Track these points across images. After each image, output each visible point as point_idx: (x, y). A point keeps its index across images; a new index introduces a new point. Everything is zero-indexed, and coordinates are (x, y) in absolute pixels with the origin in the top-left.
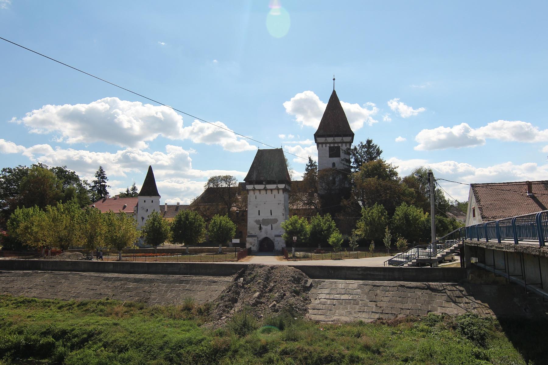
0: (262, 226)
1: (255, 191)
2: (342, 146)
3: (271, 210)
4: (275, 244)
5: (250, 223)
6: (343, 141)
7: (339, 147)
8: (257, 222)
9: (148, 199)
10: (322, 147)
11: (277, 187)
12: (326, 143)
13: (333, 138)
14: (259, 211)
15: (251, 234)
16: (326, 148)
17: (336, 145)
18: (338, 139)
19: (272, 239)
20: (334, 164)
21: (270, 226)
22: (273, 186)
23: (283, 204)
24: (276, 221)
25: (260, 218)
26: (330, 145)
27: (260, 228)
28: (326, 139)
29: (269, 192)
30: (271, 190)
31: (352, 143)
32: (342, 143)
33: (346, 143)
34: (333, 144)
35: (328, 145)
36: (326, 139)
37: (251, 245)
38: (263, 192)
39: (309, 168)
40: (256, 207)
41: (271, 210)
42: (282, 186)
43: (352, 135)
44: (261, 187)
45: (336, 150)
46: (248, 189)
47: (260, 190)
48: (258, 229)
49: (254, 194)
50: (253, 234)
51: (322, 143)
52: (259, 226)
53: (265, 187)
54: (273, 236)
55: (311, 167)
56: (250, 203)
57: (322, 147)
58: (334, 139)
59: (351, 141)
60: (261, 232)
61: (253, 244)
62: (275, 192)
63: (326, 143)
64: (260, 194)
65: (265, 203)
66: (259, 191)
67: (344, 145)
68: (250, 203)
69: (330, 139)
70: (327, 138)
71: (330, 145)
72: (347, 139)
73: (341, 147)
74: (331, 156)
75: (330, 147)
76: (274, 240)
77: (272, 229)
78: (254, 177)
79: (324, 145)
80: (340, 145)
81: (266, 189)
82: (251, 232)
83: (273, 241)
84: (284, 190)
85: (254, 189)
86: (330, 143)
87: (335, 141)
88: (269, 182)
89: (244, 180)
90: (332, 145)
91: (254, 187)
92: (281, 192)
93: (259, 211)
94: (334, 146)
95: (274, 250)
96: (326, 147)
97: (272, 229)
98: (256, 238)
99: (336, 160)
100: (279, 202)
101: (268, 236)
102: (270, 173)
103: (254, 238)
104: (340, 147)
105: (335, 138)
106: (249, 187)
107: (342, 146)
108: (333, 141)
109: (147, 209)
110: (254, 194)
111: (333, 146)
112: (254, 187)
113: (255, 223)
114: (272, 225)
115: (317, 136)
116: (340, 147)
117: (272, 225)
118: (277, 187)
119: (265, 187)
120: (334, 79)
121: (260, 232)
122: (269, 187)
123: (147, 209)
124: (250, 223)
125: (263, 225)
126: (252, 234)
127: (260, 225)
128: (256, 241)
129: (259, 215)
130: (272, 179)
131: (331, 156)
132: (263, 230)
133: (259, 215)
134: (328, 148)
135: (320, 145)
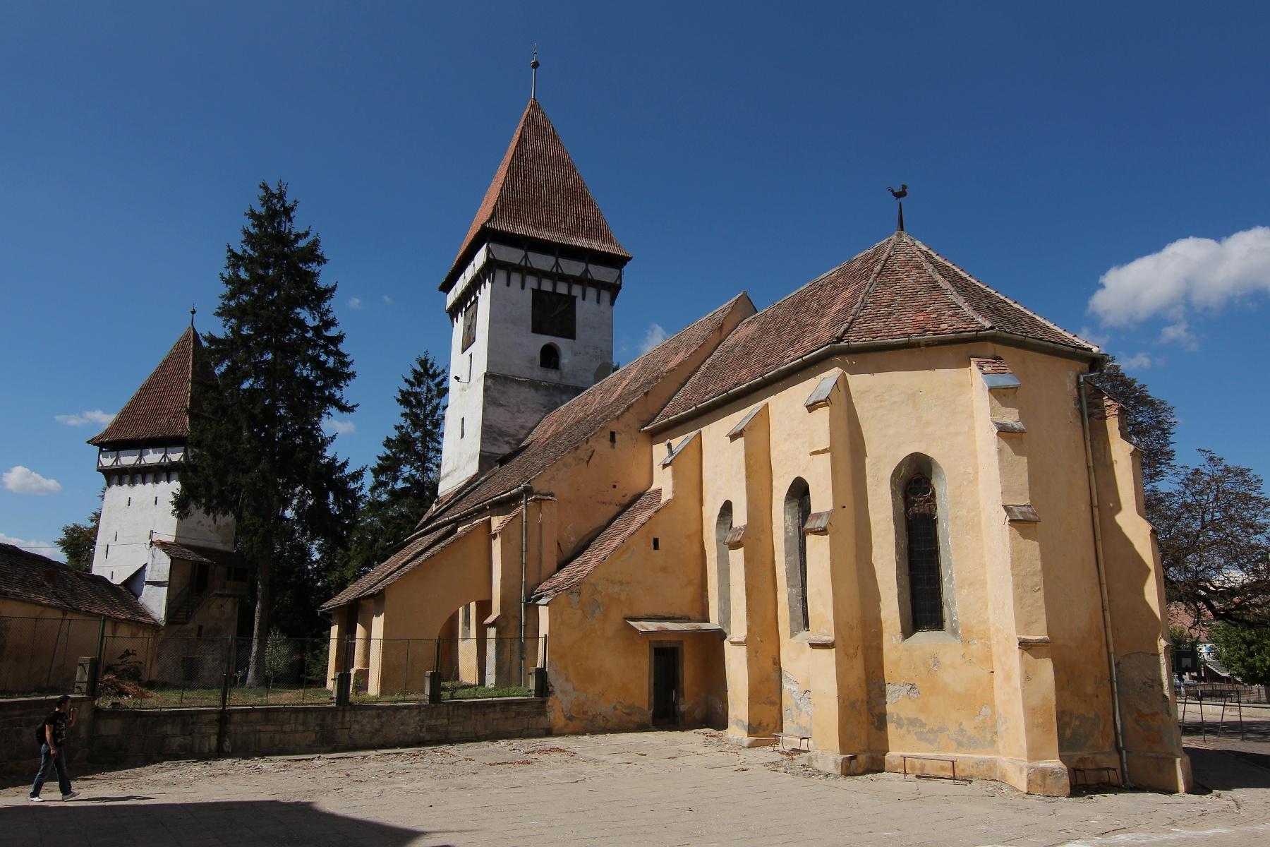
7: (571, 300)
12: (525, 271)
17: (562, 289)
26: (539, 284)
32: (585, 281)
35: (532, 282)
67: (591, 292)
69: (542, 262)
70: (531, 255)
71: (539, 284)
73: (579, 301)
75: (537, 293)
80: (577, 290)
86: (540, 274)
90: (547, 286)
94: (554, 292)
104: (575, 297)
116: (575, 297)
134: (528, 294)
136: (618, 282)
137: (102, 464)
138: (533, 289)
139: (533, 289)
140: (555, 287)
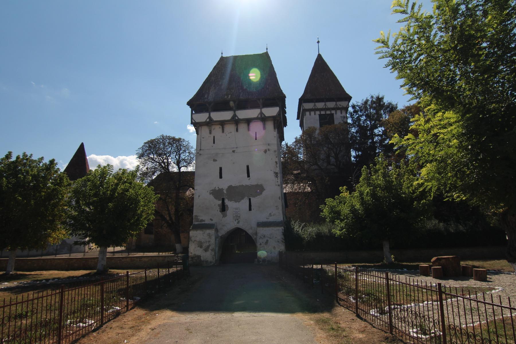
0: (227, 202)
1: (213, 127)
2: (336, 114)
3: (248, 167)
5: (199, 196)
6: (337, 106)
7: (332, 115)
8: (217, 193)
10: (310, 115)
11: (261, 113)
12: (315, 110)
13: (323, 104)
14: (221, 169)
15: (202, 221)
17: (328, 112)
18: (331, 105)
19: (250, 232)
21: (245, 203)
22: (253, 113)
23: (275, 151)
24: (258, 189)
25: (224, 184)
26: (320, 113)
27: (223, 208)
29: (243, 127)
32: (336, 109)
34: (324, 111)
35: (318, 113)
36: (315, 105)
38: (230, 128)
40: (215, 160)
41: (248, 167)
44: (227, 115)
45: (328, 118)
46: (197, 121)
47: (222, 123)
48: (218, 208)
49: (210, 133)
50: (207, 222)
52: (220, 202)
53: (235, 116)
54: (254, 225)
57: (310, 115)
58: (325, 105)
60: (225, 216)
61: (205, 245)
64: (223, 132)
66: (221, 127)
67: (339, 112)
69: (320, 105)
71: (320, 113)
72: (343, 104)
73: (335, 115)
75: (320, 115)
76: (256, 234)
77: (250, 209)
78: (211, 96)
79: (312, 113)
80: (333, 112)
81: (236, 121)
82: (201, 218)
83: (254, 237)
86: (320, 110)
87: (327, 107)
88: (243, 105)
89: (189, 103)
90: (323, 113)
91: (210, 117)
93: (221, 169)
94: (326, 114)
95: (256, 260)
97: (250, 209)
98: (212, 232)
101: (241, 225)
103: (208, 231)
104: (333, 114)
105: (326, 103)
107: (336, 114)
108: (324, 107)
110: (210, 133)
111: (324, 113)
112: (210, 117)
113: (212, 197)
114: (250, 200)
117: (250, 200)
118: (261, 113)
119: (235, 116)
120: (318, 42)
121: (222, 215)
124: (199, 196)
125: (230, 200)
126: (204, 221)
127: (223, 200)
128: (213, 238)
129: (221, 177)
132: (229, 212)
133: (221, 177)
134: (317, 117)
136: (348, 106)
137: (194, 120)
138: (319, 115)
139: (319, 115)
140: (326, 112)
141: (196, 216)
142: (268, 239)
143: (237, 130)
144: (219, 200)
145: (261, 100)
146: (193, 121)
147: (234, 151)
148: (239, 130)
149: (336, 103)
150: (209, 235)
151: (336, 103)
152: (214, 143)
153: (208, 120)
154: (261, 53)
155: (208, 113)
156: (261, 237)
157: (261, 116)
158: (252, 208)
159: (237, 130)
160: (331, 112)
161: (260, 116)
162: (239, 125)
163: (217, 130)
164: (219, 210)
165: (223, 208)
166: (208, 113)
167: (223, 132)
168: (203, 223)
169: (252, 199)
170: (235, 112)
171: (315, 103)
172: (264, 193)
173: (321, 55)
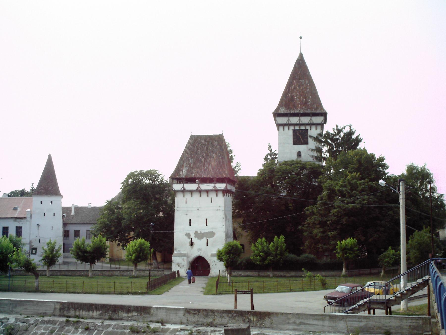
0: (194, 240)
2: (311, 130)
4: (211, 267)
7: (306, 131)
9: (46, 199)
10: (284, 130)
11: (215, 187)
12: (289, 125)
14: (190, 220)
16: (289, 133)
17: (303, 128)
18: (305, 120)
20: (299, 154)
24: (212, 234)
25: (191, 231)
26: (294, 128)
27: (192, 244)
28: (289, 120)
30: (207, 192)
31: (325, 123)
32: (311, 124)
33: (316, 125)
35: (292, 128)
36: (289, 120)
37: (179, 266)
38: (196, 195)
39: (269, 157)
40: (186, 214)
42: (221, 186)
43: (324, 115)
46: (175, 189)
47: (191, 192)
49: (184, 197)
51: (284, 125)
52: (190, 240)
53: (199, 187)
54: (210, 255)
55: (271, 156)
56: (178, 209)
57: (284, 130)
58: (300, 119)
59: (323, 122)
60: (192, 248)
62: (212, 195)
63: (289, 125)
64: (192, 196)
65: (198, 209)
66: (190, 193)
67: (313, 128)
68: (178, 209)
69: (294, 120)
74: (295, 143)
75: (294, 131)
77: (207, 245)
79: (286, 128)
80: (308, 127)
81: (199, 191)
84: (225, 192)
85: (184, 191)
88: (204, 181)
90: (297, 128)
91: (183, 187)
92: (220, 194)
93: (190, 220)
94: (300, 130)
96: (289, 130)
97: (207, 245)
98: (185, 258)
99: (302, 148)
100: (218, 208)
102: (205, 168)
103: (183, 258)
104: (308, 130)
106: (177, 187)
107: (311, 130)
109: (44, 214)
110: (184, 197)
112: (183, 187)
114: (207, 239)
115: (277, 114)
116: (308, 130)
117: (207, 239)
118: (215, 187)
119: (199, 187)
120: (301, 38)
121: (191, 248)
122: (204, 187)
123: (44, 214)
127: (192, 239)
128: (186, 261)
129: (190, 225)
130: (208, 176)
131: (295, 143)
132: (195, 246)
133: (190, 225)
134: (291, 132)
135: (281, 128)
138: (293, 130)
139: (293, 130)
140: (300, 128)
141: (176, 248)
142: (217, 263)
143: (200, 196)
144: (189, 239)
145: (215, 179)
146: (173, 189)
147: (198, 209)
148: (201, 196)
149: (311, 118)
150: (183, 260)
151: (311, 118)
152: (186, 203)
153: (182, 189)
154: (219, 134)
155: (182, 185)
156: (213, 262)
157: (215, 188)
158: (208, 244)
159: (200, 196)
160: (305, 128)
161: (214, 189)
162: (201, 193)
163: (188, 196)
164: (189, 245)
165: (192, 244)
166: (182, 185)
167: (192, 196)
168: (180, 252)
169: (208, 239)
170: (199, 185)
171: (289, 117)
172: (215, 236)
173: (302, 55)
